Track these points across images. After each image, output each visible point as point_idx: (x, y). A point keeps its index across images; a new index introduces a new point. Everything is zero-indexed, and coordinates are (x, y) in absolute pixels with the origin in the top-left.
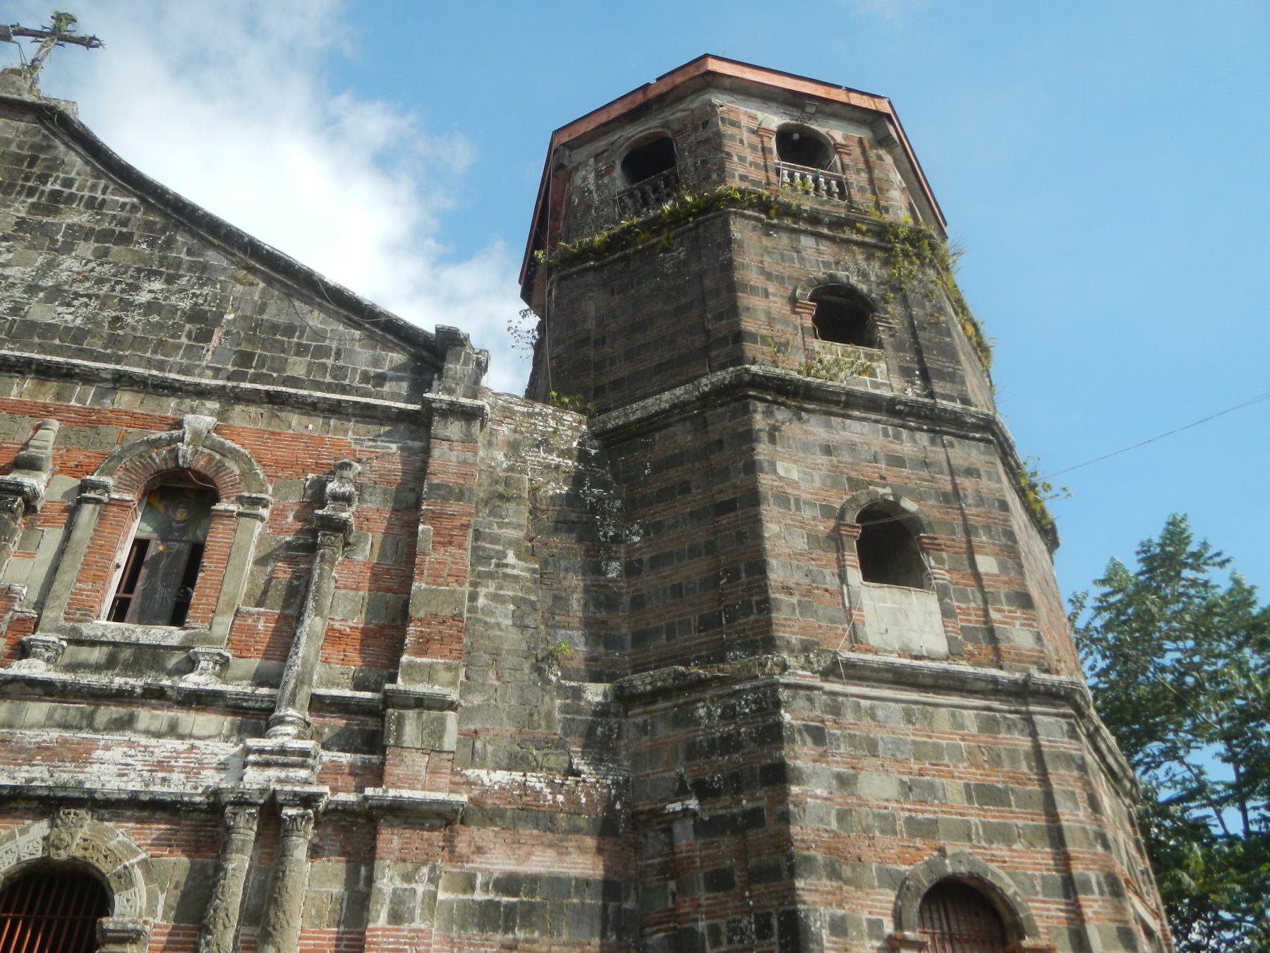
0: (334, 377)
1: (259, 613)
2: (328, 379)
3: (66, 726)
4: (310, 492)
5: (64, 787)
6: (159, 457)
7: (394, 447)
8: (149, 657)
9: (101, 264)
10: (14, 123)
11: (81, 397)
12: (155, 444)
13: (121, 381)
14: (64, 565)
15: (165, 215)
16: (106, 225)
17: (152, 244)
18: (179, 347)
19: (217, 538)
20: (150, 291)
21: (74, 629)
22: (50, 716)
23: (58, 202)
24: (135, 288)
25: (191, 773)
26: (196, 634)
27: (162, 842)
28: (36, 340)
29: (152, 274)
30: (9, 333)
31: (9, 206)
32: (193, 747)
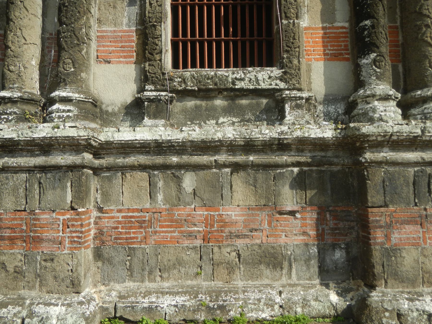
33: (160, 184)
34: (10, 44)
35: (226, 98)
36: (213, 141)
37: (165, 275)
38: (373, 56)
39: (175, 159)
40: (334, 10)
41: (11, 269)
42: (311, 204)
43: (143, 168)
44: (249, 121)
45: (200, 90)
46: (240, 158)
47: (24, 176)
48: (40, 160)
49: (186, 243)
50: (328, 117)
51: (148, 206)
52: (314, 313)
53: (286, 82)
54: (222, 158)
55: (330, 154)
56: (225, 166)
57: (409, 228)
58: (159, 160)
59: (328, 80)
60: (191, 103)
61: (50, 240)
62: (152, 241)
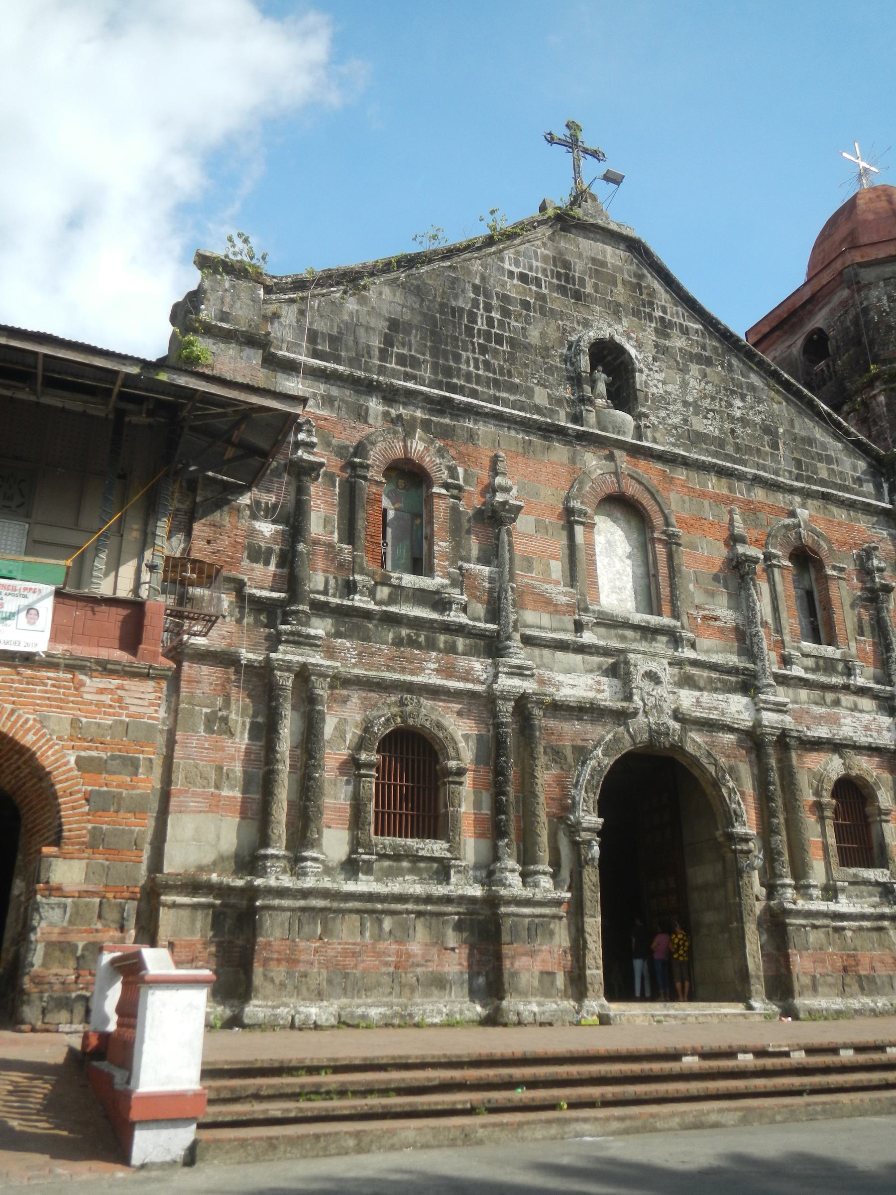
0: (841, 479)
1: (865, 641)
2: (839, 482)
3: (816, 704)
4: (858, 562)
5: (845, 739)
6: (792, 535)
7: (885, 532)
8: (828, 665)
9: (707, 383)
10: (617, 251)
11: (740, 491)
12: (787, 527)
13: (757, 480)
14: (781, 608)
15: (719, 341)
16: (696, 350)
17: (723, 367)
18: (766, 453)
19: (834, 593)
20: (739, 408)
21: (799, 649)
22: (809, 698)
23: (666, 327)
24: (730, 405)
25: (879, 731)
26: (844, 653)
27: (880, 767)
28: (704, 446)
29: (733, 392)
30: (689, 440)
31: (645, 330)
32: (875, 719)
33: (368, 924)
34: (274, 812)
35: (410, 861)
36: (407, 895)
37: (369, 994)
38: (506, 840)
39: (379, 906)
40: (481, 801)
41: (277, 981)
42: (465, 943)
43: (358, 911)
44: (425, 879)
45: (394, 854)
46: (422, 907)
47: (288, 914)
48: (302, 903)
49: (384, 969)
50: (476, 880)
51: (359, 940)
52: (467, 1019)
53: (451, 853)
54: (410, 906)
55: (477, 907)
56: (412, 912)
57: (524, 959)
58: (369, 906)
59: (476, 853)
60: (386, 863)
61: (304, 962)
62: (361, 966)
